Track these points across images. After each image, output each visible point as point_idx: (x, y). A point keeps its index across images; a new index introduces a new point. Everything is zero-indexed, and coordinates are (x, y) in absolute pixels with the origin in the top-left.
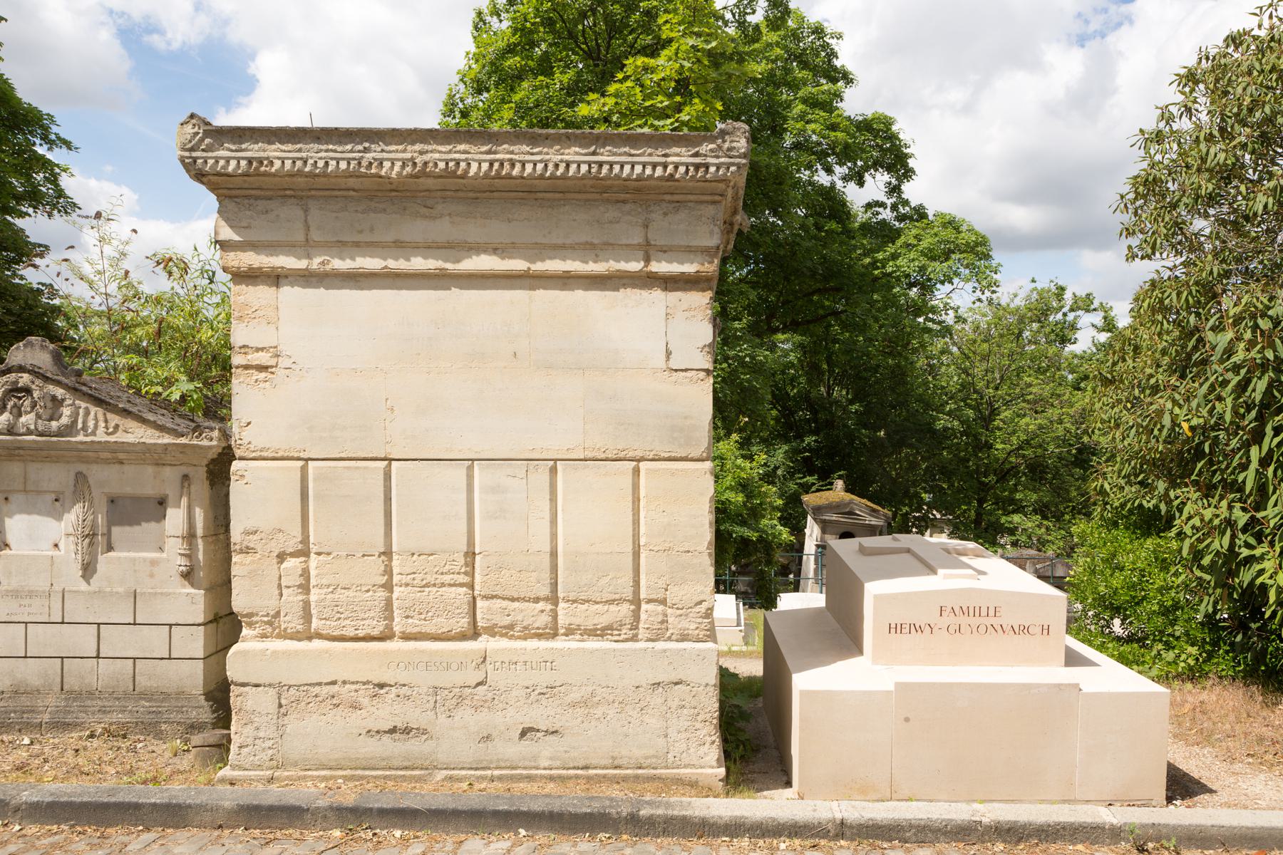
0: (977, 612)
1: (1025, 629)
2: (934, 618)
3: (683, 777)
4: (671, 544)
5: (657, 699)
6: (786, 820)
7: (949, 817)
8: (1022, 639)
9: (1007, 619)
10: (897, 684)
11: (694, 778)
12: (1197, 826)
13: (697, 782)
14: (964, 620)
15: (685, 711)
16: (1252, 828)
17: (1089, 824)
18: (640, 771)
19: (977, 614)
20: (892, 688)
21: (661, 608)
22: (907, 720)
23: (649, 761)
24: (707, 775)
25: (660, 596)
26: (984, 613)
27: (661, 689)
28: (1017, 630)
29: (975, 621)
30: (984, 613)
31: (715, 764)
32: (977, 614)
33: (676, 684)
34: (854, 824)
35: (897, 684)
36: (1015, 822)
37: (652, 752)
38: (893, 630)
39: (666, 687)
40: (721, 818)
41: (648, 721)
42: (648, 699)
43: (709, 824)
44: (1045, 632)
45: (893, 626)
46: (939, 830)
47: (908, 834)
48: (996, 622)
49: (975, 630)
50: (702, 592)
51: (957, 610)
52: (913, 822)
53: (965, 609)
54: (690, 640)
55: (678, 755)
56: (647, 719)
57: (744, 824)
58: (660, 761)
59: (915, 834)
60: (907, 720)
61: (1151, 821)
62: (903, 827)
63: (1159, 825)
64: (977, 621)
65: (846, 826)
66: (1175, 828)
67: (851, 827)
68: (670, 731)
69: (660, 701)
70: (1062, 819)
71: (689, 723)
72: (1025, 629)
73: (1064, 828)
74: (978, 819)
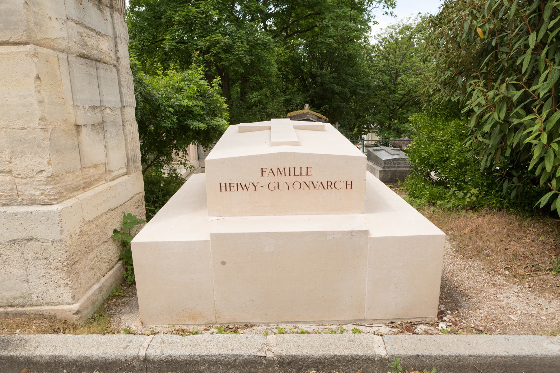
0: (292, 172)
1: (333, 185)
2: (256, 177)
3: (44, 313)
4: (7, 123)
5: (15, 253)
6: (96, 358)
7: (238, 353)
8: (331, 192)
9: (317, 177)
10: (212, 235)
11: (52, 313)
12: (456, 356)
13: (55, 316)
14: (281, 179)
15: (40, 262)
16: (505, 357)
17: (360, 356)
18: (10, 309)
19: (292, 173)
20: (208, 238)
21: (8, 178)
22: (223, 263)
23: (17, 300)
24: (66, 311)
25: (6, 168)
26: (298, 172)
27: (17, 245)
28: (325, 186)
29: (290, 179)
30: (298, 172)
31: (70, 301)
32: (292, 173)
33: (29, 240)
34: (155, 360)
35: (212, 235)
36: (295, 356)
37: (18, 294)
38: (223, 189)
39: (21, 243)
40: (41, 357)
41: (11, 270)
42: (7, 253)
43: (33, 362)
44: (349, 186)
45: (223, 185)
46: (229, 364)
47: (202, 368)
48: (308, 179)
49: (291, 187)
50: (40, 163)
51: (275, 171)
52: (206, 358)
53: (282, 169)
54: (39, 204)
55: (40, 295)
56: (9, 268)
57: (62, 362)
58: (26, 301)
59: (208, 367)
60: (223, 263)
61: (415, 353)
62: (198, 362)
63: (423, 356)
64: (292, 179)
65: (149, 361)
66: (436, 358)
67: (153, 362)
68: (30, 277)
69: (17, 254)
70: (337, 353)
71: (45, 271)
72: (333, 185)
73: (339, 361)
74: (263, 354)
